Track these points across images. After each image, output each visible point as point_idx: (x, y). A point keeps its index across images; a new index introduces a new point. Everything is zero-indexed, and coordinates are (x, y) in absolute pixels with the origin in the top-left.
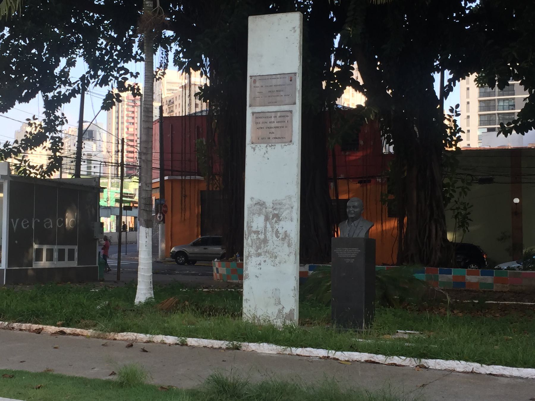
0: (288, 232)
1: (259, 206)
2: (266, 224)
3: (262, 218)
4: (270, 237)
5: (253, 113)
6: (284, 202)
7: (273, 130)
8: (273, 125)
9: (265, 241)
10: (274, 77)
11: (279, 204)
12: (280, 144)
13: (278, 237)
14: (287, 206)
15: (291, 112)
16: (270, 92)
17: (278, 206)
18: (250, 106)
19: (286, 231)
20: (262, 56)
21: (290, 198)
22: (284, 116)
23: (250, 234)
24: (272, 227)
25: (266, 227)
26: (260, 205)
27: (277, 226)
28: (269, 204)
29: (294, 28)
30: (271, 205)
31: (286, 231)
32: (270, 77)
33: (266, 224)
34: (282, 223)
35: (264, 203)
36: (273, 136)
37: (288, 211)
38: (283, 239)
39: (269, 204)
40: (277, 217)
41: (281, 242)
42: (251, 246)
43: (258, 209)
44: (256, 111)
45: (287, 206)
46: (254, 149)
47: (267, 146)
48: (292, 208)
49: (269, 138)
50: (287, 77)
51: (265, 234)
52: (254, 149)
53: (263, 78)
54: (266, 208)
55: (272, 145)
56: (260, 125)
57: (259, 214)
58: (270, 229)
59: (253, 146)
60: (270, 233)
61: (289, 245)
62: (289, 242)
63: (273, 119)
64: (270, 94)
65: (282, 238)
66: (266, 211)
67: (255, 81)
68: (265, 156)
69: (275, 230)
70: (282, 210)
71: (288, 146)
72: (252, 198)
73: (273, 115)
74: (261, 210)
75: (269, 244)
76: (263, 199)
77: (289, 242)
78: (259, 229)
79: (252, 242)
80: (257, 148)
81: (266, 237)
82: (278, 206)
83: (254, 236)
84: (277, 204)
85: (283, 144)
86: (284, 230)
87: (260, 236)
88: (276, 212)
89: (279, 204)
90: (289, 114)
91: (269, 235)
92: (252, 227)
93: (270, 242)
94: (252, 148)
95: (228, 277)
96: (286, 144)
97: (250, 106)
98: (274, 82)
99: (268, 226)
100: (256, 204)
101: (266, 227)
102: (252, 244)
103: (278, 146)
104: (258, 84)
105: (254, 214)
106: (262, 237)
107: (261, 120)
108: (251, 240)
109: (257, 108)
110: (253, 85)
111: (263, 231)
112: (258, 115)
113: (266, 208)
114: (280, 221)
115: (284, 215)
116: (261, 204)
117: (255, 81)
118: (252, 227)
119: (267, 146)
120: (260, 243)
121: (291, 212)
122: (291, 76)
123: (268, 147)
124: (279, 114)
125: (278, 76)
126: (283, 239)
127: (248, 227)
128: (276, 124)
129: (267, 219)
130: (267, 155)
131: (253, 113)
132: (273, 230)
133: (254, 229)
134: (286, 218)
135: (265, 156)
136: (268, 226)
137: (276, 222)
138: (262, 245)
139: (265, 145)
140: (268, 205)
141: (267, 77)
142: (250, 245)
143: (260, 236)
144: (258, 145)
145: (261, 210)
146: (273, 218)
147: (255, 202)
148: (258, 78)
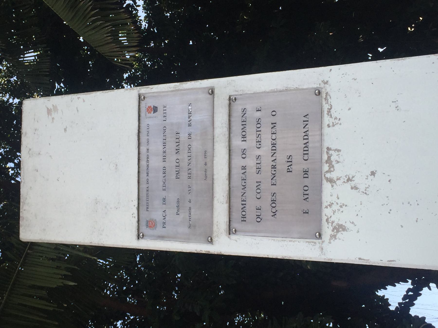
5: (231, 231)
7: (281, 158)
8: (267, 162)
10: (143, 163)
12: (326, 130)
15: (231, 100)
16: (178, 173)
18: (211, 241)
20: (97, 202)
22: (244, 124)
29: (49, 112)
32: (143, 175)
44: (226, 219)
46: (339, 228)
47: (331, 181)
49: (306, 172)
50: (150, 122)
52: (339, 228)
55: (329, 161)
56: (266, 204)
59: (327, 231)
63: (251, 163)
64: (184, 175)
67: (151, 224)
68: (362, 188)
71: (333, 101)
73: (238, 162)
80: (338, 218)
85: (327, 120)
90: (238, 108)
94: (333, 237)
96: (326, 107)
97: (211, 241)
98: (156, 162)
103: (332, 137)
104: (157, 216)
107: (252, 204)
109: (215, 220)
110: (159, 231)
112: (237, 215)
117: (151, 224)
119: (331, 181)
123: (333, 175)
124: (237, 142)
125: (143, 149)
131: (231, 231)
135: (362, 188)
139: (326, 186)
141: (144, 186)
144: (327, 212)
148: (144, 215)
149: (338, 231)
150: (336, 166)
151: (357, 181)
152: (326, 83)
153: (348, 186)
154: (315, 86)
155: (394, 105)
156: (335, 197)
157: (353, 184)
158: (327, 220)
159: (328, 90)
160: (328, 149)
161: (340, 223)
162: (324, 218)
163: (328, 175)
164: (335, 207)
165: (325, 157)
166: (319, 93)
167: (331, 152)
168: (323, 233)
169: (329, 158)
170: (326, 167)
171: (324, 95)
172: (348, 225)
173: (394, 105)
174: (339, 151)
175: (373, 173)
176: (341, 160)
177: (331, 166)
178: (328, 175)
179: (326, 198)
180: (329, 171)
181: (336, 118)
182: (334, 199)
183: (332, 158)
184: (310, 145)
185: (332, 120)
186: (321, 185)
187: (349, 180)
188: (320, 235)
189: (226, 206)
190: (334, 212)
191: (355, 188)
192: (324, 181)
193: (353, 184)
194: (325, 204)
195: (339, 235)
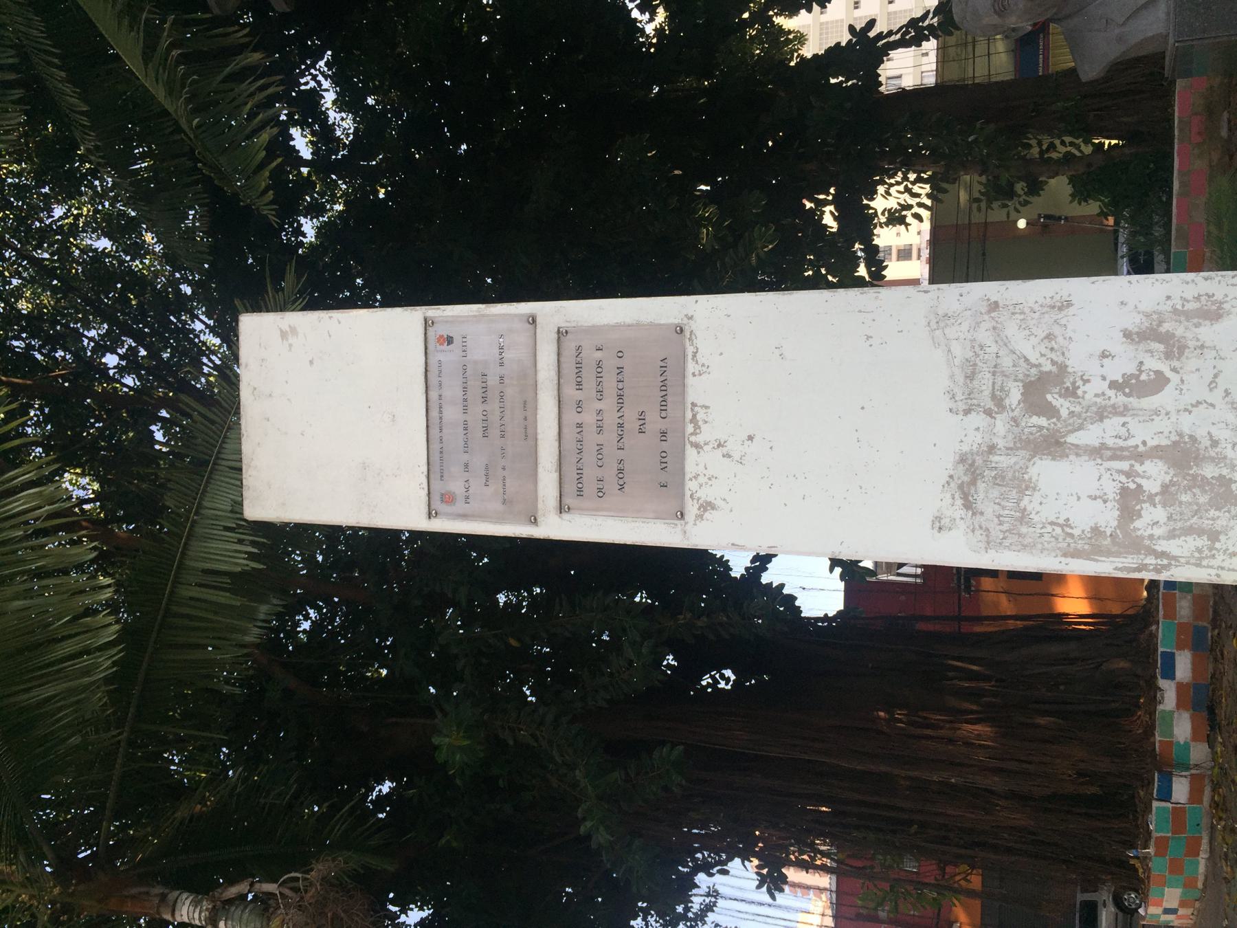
0: (1133, 321)
1: (981, 486)
2: (1079, 450)
3: (1045, 471)
4: (1161, 424)
5: (562, 509)
6: (960, 351)
7: (631, 416)
8: (611, 419)
9: (1182, 453)
10: (434, 413)
11: (971, 377)
12: (690, 380)
13: (1160, 382)
14: (984, 335)
15: (561, 334)
16: (486, 429)
17: (985, 382)
18: (534, 522)
19: (1127, 335)
20: (365, 466)
21: (942, 320)
22: (579, 368)
23: (1136, 545)
24: (1101, 415)
25: (1097, 452)
26: (973, 482)
27: (1092, 390)
28: (971, 432)
29: (284, 335)
30: (978, 419)
31: (1127, 335)
32: (435, 432)
33: (1079, 450)
34: (1078, 360)
35: (962, 459)
36: (653, 417)
37: (1011, 329)
38: (1174, 348)
39: (971, 432)
40: (1041, 387)
41: (1191, 362)
42: (1214, 536)
43: (995, 493)
44: (556, 493)
45: (984, 335)
46: (707, 506)
47: (696, 446)
48: (995, 306)
49: (664, 434)
50: (441, 357)
51: (1140, 457)
52: (707, 506)
53: (435, 468)
54: (992, 449)
55: (694, 419)
56: (610, 473)
57: (1025, 487)
58: (1113, 425)
59: (692, 509)
60: (1133, 424)
61: (1213, 313)
62: (1188, 315)
63: (589, 418)
64: (495, 432)
65: (1168, 356)
66: (1010, 450)
67: (448, 498)
68: (736, 456)
69: (1121, 399)
70: (1007, 362)
71: (699, 342)
72: (939, 525)
73: (571, 417)
74: (999, 479)
75: (1201, 433)
76: (944, 464)
77: (1188, 315)
78: (1111, 488)
79: (1189, 531)
80: (705, 494)
81: (1157, 452)
82: (985, 382)
83: (1152, 518)
84: (974, 390)
85: (691, 367)
86: (1117, 345)
87: (1151, 486)
88: (1015, 395)
89: (971, 377)
90: (570, 345)
91: (1144, 434)
92: (1096, 530)
93: (1186, 424)
94: (700, 517)
95: (1189, 884)
96: (690, 350)
97: (534, 522)
98: (452, 414)
99: (1090, 436)
100: (968, 505)
101: (1097, 452)
102: (1200, 532)
103: (697, 389)
104: (457, 487)
105: (1023, 517)
106: (1155, 474)
107: (590, 473)
108: (1172, 535)
109: (541, 493)
110: (460, 507)
111: (1125, 465)
112: (570, 488)
113: (992, 449)
114: (1063, 368)
115: (1030, 348)
116: (971, 474)
117: (448, 498)
118: (1096, 530)
119: (696, 446)
120: (1200, 483)
121: (1016, 309)
122: (435, 341)
125: (434, 395)
126: (1174, 348)
127: (1094, 552)
128: (609, 404)
129: (1052, 445)
130: (733, 447)
131: (562, 509)
132: (1116, 411)
133: (1108, 517)
134: (1050, 337)
135: (736, 456)
136: (1090, 436)
137: (1071, 393)
138: (1209, 471)
139: (691, 453)
140: (973, 441)
141: (435, 446)
142: (1202, 542)
143: (1151, 486)
144: (691, 486)
145: (999, 479)
146: (1050, 412)
147: (959, 511)
148: (437, 486)
149: (705, 510)
150: (704, 427)
151: (730, 446)
152: (691, 318)
153: (719, 452)
154: (676, 321)
155: (777, 352)
156: (701, 467)
157: (725, 450)
158: (691, 496)
159: (693, 327)
160: (694, 405)
161: (709, 500)
162: (688, 493)
163: (693, 439)
164: (702, 479)
165: (689, 415)
166: (682, 330)
167: (696, 409)
168: (686, 512)
169: (694, 416)
170: (690, 428)
171: (687, 334)
172: (719, 503)
173: (777, 352)
174: (707, 407)
175: (750, 438)
176: (709, 419)
177: (697, 427)
178: (693, 439)
179: (691, 467)
180: (694, 433)
181: (703, 365)
182: (701, 468)
183: (698, 417)
184: (669, 398)
185: (698, 368)
186: (684, 451)
187: (720, 445)
188: (682, 514)
189: (555, 476)
190: (701, 486)
191: (727, 456)
192: (688, 446)
193: (725, 450)
194: (688, 477)
195: (707, 515)
